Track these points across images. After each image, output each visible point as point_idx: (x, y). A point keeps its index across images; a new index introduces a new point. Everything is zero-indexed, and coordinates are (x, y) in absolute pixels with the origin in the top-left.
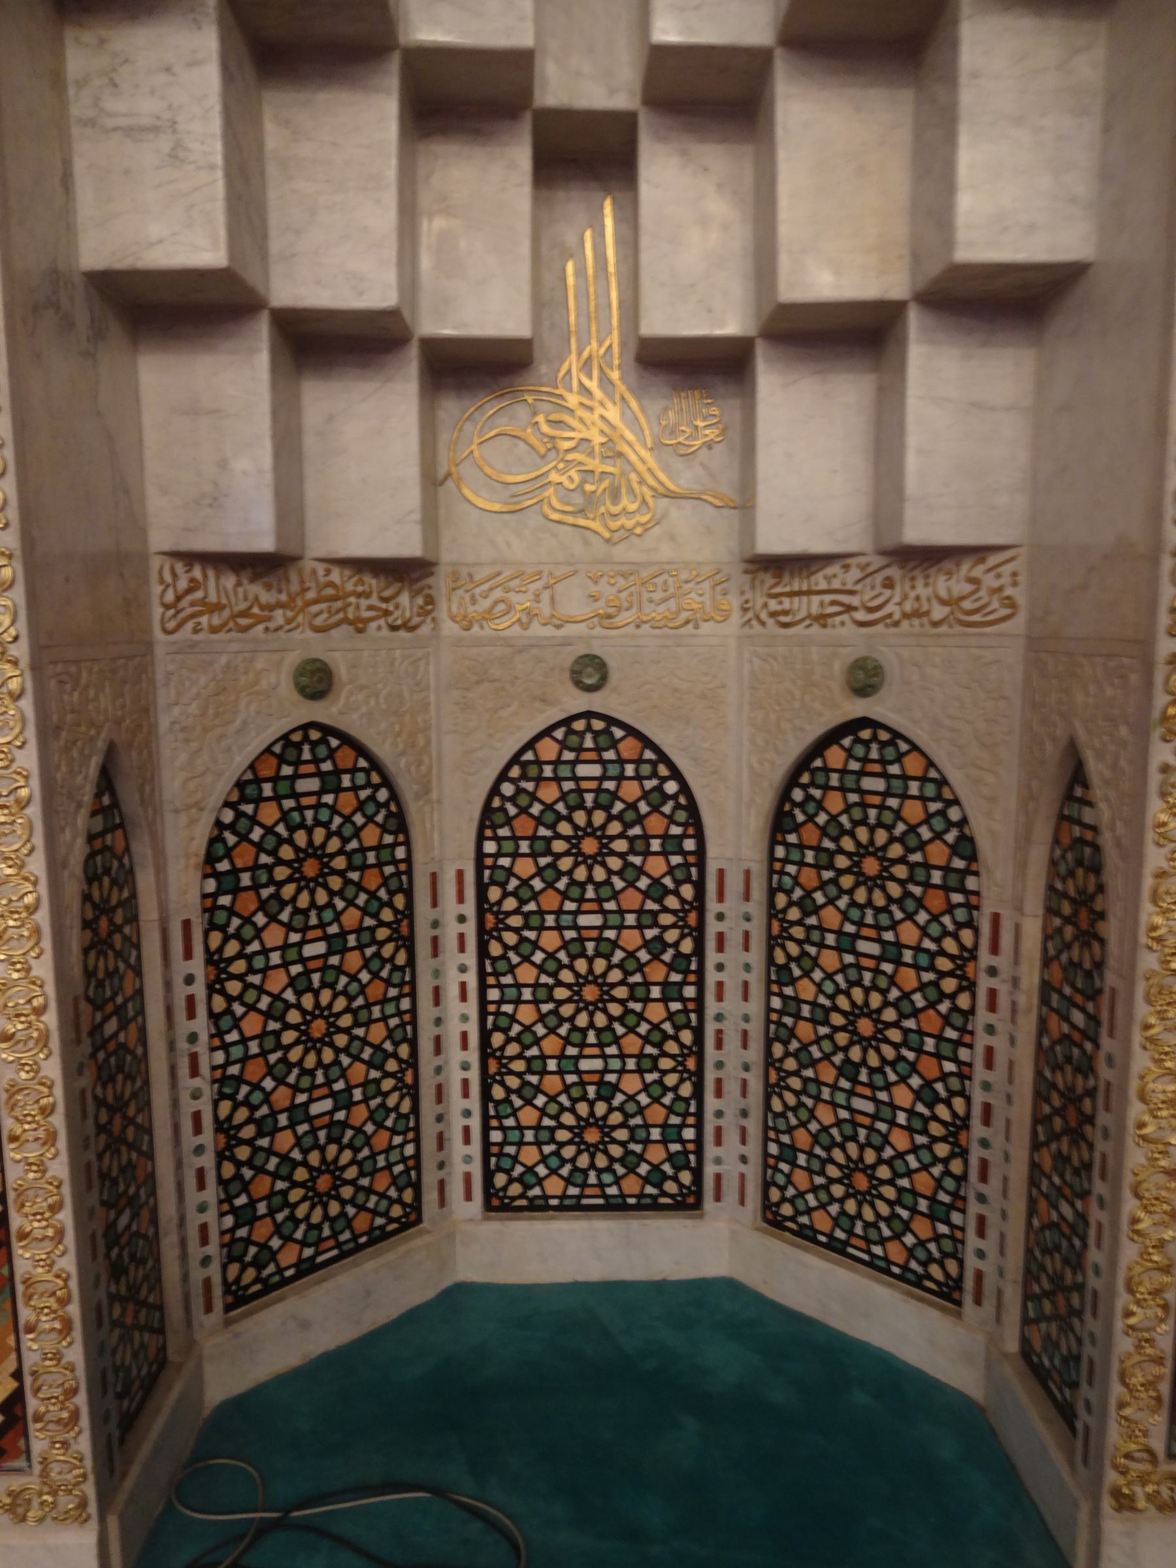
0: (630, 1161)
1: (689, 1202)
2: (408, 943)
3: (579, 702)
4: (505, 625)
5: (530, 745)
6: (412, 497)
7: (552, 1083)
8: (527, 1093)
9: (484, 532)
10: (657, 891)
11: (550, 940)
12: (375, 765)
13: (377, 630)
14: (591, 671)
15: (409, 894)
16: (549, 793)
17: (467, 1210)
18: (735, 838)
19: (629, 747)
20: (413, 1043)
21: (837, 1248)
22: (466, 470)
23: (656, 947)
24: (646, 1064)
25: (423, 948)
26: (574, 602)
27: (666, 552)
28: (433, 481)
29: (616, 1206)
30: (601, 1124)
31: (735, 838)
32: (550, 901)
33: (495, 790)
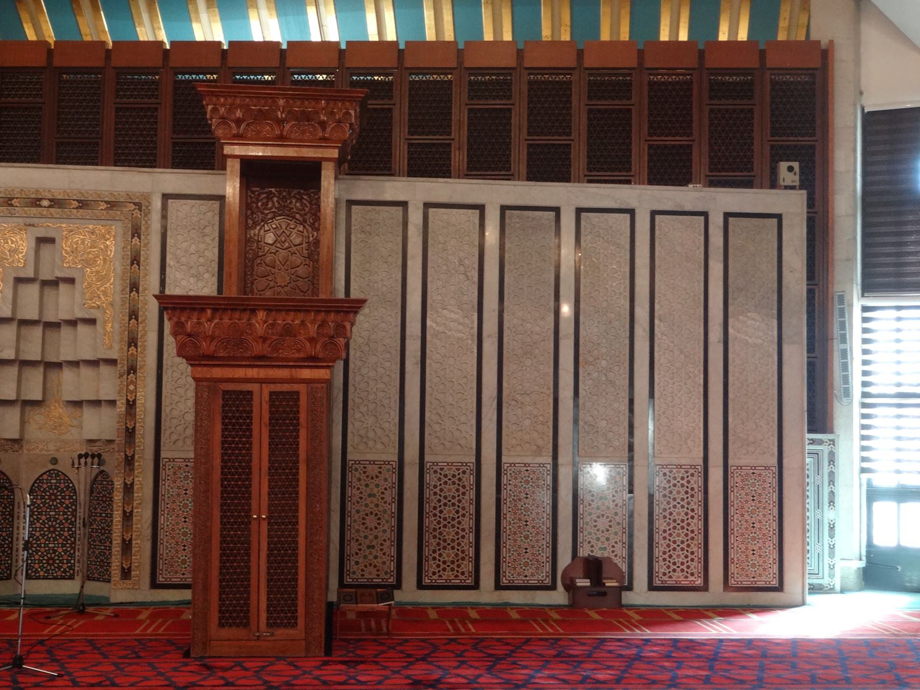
0: (59, 568)
1: (71, 578)
2: (12, 516)
3: (52, 467)
4: (37, 451)
5: (41, 476)
6: (18, 427)
7: (43, 550)
8: (37, 551)
9: (34, 432)
10: (67, 507)
11: (44, 518)
12: (8, 479)
13: (10, 451)
14: (54, 461)
15: (13, 506)
16: (45, 486)
17: (22, 577)
18: (82, 497)
19: (62, 477)
20: (12, 538)
21: (98, 580)
22: (31, 421)
23: (66, 519)
24: (63, 545)
25: (15, 517)
26: (51, 447)
27: (71, 438)
28: (23, 423)
29: (55, 578)
30: (53, 559)
31: (82, 497)
32: (44, 509)
33: (33, 485)
